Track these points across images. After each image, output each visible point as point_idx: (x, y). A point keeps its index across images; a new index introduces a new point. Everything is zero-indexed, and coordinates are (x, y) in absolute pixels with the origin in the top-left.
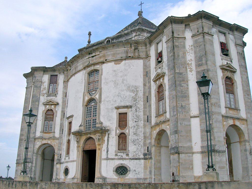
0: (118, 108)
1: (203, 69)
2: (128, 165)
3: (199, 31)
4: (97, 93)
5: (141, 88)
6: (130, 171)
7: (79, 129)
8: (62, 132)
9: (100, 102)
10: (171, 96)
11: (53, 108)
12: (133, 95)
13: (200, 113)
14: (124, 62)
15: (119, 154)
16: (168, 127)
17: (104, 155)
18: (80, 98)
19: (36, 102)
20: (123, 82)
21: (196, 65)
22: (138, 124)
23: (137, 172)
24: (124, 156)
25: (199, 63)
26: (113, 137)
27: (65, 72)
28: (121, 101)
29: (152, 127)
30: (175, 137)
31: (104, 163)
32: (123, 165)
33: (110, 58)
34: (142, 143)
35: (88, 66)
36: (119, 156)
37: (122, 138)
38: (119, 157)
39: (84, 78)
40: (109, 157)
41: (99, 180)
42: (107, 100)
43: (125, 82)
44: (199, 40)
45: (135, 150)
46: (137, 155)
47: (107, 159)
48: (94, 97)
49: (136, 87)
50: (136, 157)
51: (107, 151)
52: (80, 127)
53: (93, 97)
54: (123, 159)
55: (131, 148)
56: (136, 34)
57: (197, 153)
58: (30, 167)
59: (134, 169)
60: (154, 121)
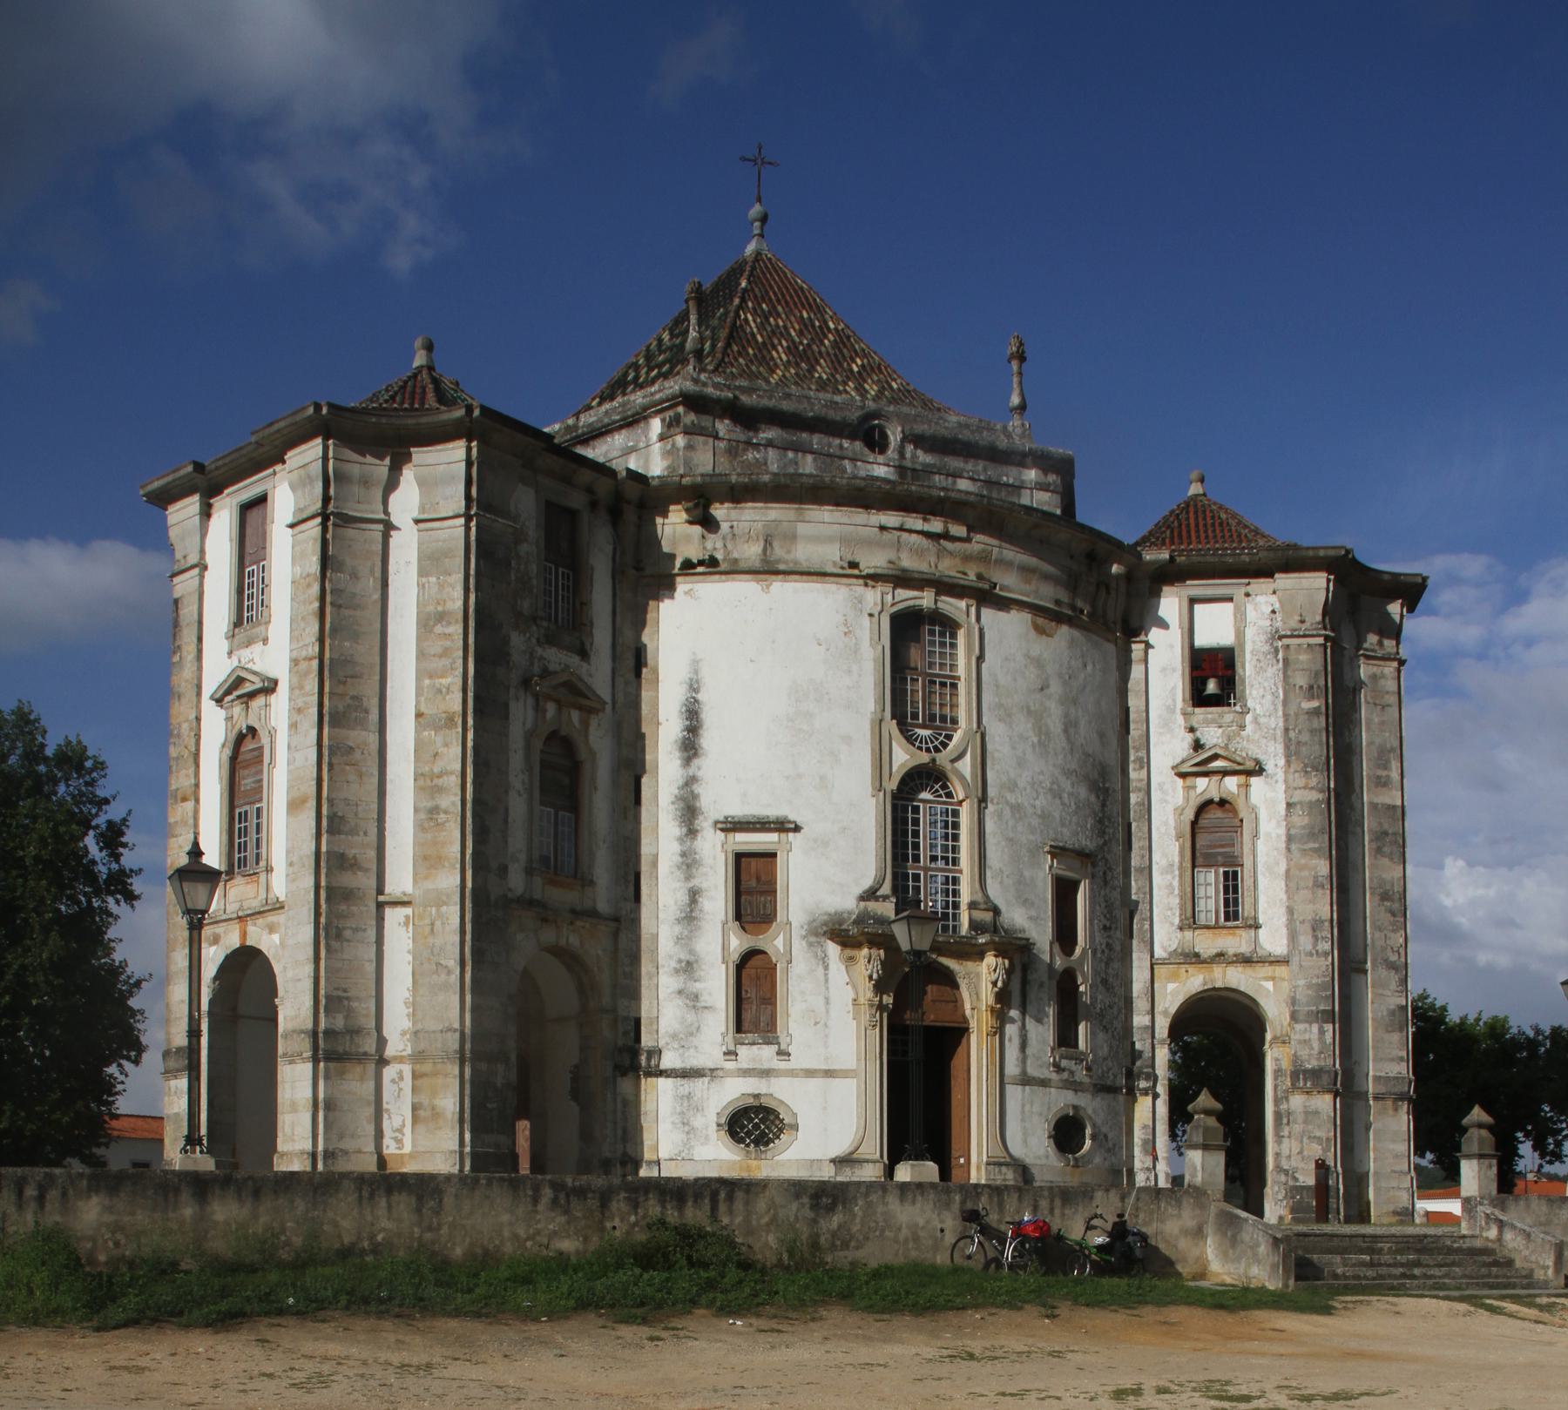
7: (861, 919)
8: (632, 889)
9: (983, 800)
10: (1305, 873)
14: (1064, 629)
18: (847, 739)
20: (1066, 731)
26: (1041, 985)
28: (1063, 825)
33: (1009, 582)
42: (1011, 798)
43: (1072, 731)
48: (948, 766)
49: (1104, 772)
52: (872, 906)
53: (943, 758)
56: (1042, 478)
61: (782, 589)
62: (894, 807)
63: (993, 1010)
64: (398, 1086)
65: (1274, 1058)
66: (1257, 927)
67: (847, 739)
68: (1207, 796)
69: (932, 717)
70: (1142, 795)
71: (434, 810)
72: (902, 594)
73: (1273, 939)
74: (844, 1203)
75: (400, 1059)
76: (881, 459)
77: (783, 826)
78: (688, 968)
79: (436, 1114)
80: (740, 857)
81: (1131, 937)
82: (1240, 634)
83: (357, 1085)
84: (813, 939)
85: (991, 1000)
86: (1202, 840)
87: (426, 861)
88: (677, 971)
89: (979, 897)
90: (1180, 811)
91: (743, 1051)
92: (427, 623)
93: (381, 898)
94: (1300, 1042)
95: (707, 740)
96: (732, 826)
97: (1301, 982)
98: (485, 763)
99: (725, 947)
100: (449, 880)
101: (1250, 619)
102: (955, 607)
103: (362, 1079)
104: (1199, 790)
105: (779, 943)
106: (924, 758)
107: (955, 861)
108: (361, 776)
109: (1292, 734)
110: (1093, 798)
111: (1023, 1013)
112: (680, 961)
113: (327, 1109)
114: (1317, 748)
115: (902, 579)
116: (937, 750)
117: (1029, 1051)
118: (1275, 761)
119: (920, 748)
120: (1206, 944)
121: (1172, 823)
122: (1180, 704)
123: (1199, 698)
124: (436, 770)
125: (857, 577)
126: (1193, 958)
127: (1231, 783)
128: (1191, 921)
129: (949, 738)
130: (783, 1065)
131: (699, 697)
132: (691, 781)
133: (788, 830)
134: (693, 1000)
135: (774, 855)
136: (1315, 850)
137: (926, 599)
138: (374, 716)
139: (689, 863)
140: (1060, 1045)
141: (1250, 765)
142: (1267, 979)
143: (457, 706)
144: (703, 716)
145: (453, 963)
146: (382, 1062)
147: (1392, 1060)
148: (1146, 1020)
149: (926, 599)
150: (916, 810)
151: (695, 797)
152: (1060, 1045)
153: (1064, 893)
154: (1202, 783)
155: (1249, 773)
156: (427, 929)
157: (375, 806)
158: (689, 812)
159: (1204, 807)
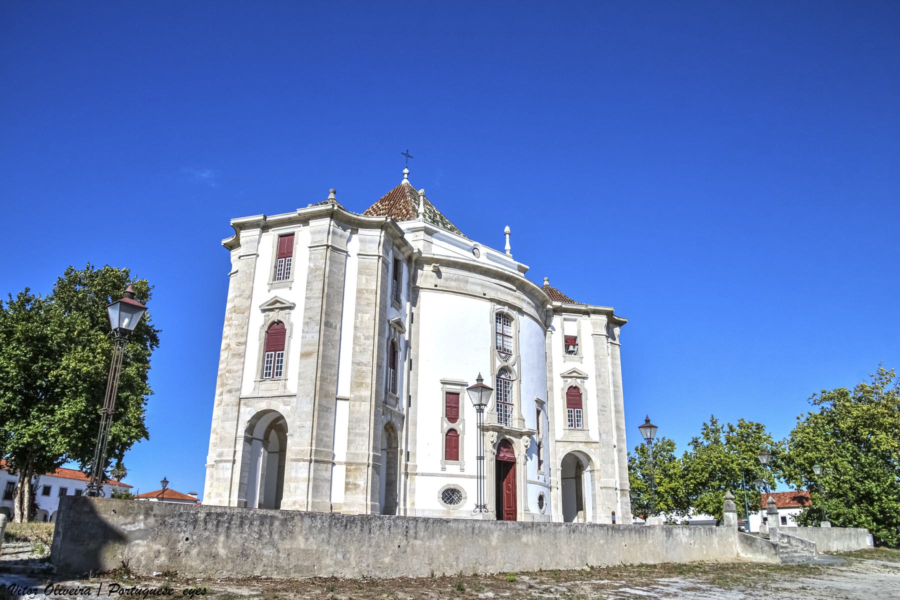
35: (499, 302)
64: (339, 474)
72: (499, 306)
75: (340, 463)
79: (356, 486)
82: (579, 332)
87: (357, 384)
90: (563, 389)
91: (447, 466)
99: (442, 426)
102: (513, 313)
105: (461, 426)
115: (499, 302)
135: (458, 394)
137: (506, 310)
149: (506, 310)
154: (570, 380)
155: (584, 378)
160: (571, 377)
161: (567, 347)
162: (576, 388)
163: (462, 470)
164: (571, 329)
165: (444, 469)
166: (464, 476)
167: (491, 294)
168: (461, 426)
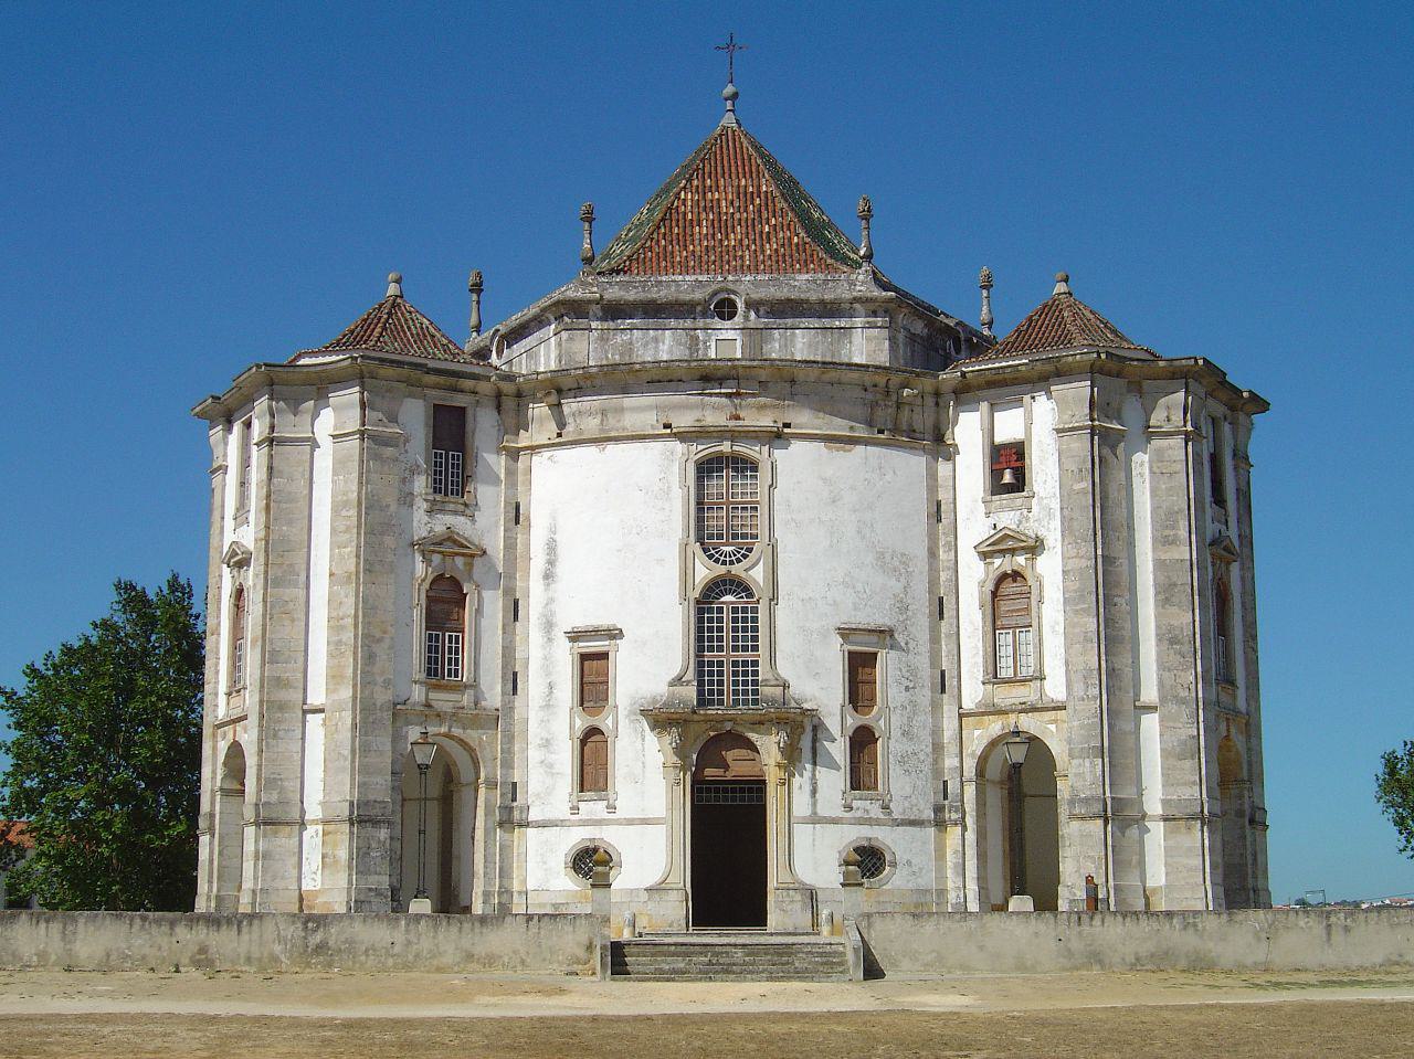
0: (846, 633)
1: (1177, 556)
2: (888, 842)
3: (1173, 418)
4: (753, 556)
5: (921, 565)
6: (894, 864)
9: (774, 598)
10: (1077, 630)
11: (461, 567)
12: (896, 586)
13: (1163, 699)
15: (856, 804)
16: (1053, 727)
17: (801, 805)
19: (382, 534)
21: (1155, 540)
22: (913, 698)
23: (915, 869)
24: (875, 811)
25: (1166, 532)
27: (509, 403)
29: (961, 716)
30: (1093, 765)
31: (802, 834)
32: (874, 843)
34: (927, 768)
36: (858, 809)
37: (862, 741)
38: (859, 814)
39: (675, 479)
40: (822, 811)
41: (788, 895)
44: (1170, 452)
45: (908, 790)
46: (914, 809)
47: (814, 819)
48: (743, 575)
49: (905, 560)
50: (912, 818)
51: (814, 792)
53: (737, 569)
54: (870, 822)
55: (901, 783)
57: (1153, 818)
58: (382, 838)
59: (906, 857)
60: (973, 691)
61: (612, 449)
62: (700, 611)
63: (779, 765)
65: (1063, 789)
66: (1042, 679)
67: (660, 561)
68: (1002, 570)
69: (735, 536)
70: (950, 573)
71: (340, 642)
73: (1055, 688)
74: (325, 926)
76: (728, 324)
77: (614, 634)
78: (547, 744)
79: (336, 862)
80: (584, 657)
81: (943, 690)
83: (284, 840)
84: (633, 718)
85: (779, 757)
86: (1004, 606)
88: (540, 746)
89: (769, 676)
90: (982, 584)
92: (336, 509)
93: (305, 707)
94: (1076, 775)
95: (560, 569)
96: (575, 636)
97: (1076, 723)
98: (368, 609)
99: (572, 727)
100: (346, 693)
101: (1042, 423)
103: (289, 836)
104: (996, 566)
105: (609, 722)
106: (721, 570)
107: (755, 648)
108: (293, 620)
109: (1066, 512)
110: (893, 582)
111: (815, 764)
112: (542, 739)
113: (262, 857)
114: (1084, 522)
116: (739, 561)
117: (817, 795)
118: (1053, 535)
119: (717, 561)
120: (1007, 696)
121: (976, 595)
122: (982, 494)
123: (997, 488)
124: (341, 614)
125: (669, 436)
126: (991, 710)
127: (1021, 560)
128: (993, 677)
129: (750, 550)
130: (611, 816)
131: (556, 537)
132: (551, 600)
133: (614, 637)
134: (548, 766)
136: (1083, 610)
138: (303, 577)
139: (548, 664)
140: (853, 788)
141: (1031, 543)
142: (1051, 722)
143: (353, 569)
144: (559, 551)
145: (347, 752)
146: (303, 824)
147: (1185, 784)
148: (956, 762)
150: (720, 610)
151: (553, 614)
152: (853, 788)
153: (860, 668)
156: (334, 728)
157: (303, 642)
158: (549, 626)
159: (1003, 578)
160: (1003, 552)
161: (995, 474)
162: (1016, 575)
163: (612, 808)
164: (1009, 426)
165: (575, 809)
166: (618, 822)
167: (683, 421)
168: (609, 722)
